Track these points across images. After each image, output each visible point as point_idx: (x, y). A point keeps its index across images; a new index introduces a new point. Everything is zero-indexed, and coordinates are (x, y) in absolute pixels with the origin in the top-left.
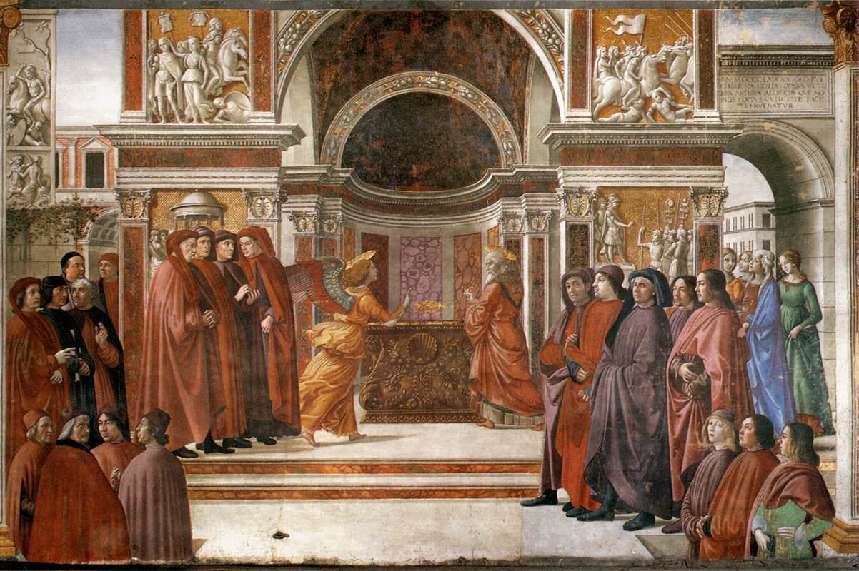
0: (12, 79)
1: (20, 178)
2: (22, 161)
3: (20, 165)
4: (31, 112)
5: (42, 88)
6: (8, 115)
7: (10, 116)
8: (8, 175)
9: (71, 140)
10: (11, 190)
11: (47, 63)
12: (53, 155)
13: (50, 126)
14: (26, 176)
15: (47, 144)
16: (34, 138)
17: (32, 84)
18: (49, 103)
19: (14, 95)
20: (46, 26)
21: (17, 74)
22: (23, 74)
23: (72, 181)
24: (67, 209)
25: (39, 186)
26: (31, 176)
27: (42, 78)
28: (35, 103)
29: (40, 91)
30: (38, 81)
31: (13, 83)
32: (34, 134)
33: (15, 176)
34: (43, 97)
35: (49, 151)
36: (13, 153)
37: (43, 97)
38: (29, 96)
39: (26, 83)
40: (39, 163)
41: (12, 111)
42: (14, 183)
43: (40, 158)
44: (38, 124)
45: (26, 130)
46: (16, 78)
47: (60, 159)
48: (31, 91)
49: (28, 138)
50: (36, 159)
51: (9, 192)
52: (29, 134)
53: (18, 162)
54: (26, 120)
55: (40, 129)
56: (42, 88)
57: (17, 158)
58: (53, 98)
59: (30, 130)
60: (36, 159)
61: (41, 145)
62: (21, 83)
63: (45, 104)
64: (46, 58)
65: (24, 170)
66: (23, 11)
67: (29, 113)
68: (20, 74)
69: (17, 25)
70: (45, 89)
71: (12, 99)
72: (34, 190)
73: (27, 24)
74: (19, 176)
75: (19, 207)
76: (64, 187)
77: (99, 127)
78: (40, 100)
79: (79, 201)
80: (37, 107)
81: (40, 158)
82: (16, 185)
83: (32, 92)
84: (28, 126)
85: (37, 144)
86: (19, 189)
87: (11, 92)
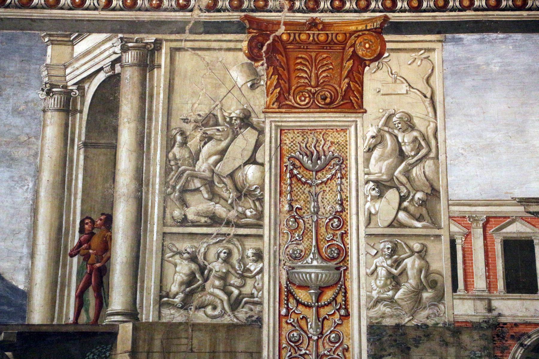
0: (372, 131)
1: (391, 276)
2: (394, 251)
3: (391, 256)
4: (408, 178)
5: (423, 143)
6: (367, 182)
7: (371, 184)
8: (369, 271)
9: (474, 219)
10: (375, 294)
11: (430, 109)
12: (444, 246)
13: (439, 198)
14: (401, 274)
15: (435, 224)
16: (412, 216)
17: (406, 138)
18: (437, 167)
19: (376, 153)
20: (427, 58)
21: (380, 124)
22: (391, 125)
23: (480, 283)
24: (473, 326)
25: (424, 289)
26: (410, 273)
27: (423, 129)
28: (413, 165)
29: (420, 148)
30: (415, 134)
31: (373, 137)
32: (412, 209)
33: (382, 272)
34: (425, 156)
35: (438, 237)
36: (377, 239)
37: (425, 156)
38: (402, 156)
39: (396, 137)
40: (422, 254)
41: (372, 177)
42: (380, 283)
43: (424, 246)
44: (419, 195)
45: (400, 204)
46: (379, 130)
47: (459, 248)
48: (403, 148)
49: (402, 216)
50: (417, 246)
51: (369, 297)
52: (406, 210)
53: (387, 252)
54: (398, 189)
55: (423, 203)
56: (423, 143)
57: (385, 245)
58: (442, 157)
59: (406, 204)
60: (417, 246)
61: (424, 227)
62: (388, 136)
63: (429, 164)
64: (428, 101)
65: (397, 263)
66: (387, 37)
67: (403, 179)
68: (386, 124)
69: (379, 56)
70: (428, 145)
71: (373, 161)
72: (417, 292)
73: (393, 55)
74: (389, 273)
75: (388, 322)
76: (466, 288)
77: (525, 201)
78: (420, 160)
79: (495, 313)
80: (416, 171)
81: (424, 246)
82: (385, 285)
83: (406, 149)
84: (402, 199)
85: (419, 224)
86: (390, 293)
87: (370, 150)
